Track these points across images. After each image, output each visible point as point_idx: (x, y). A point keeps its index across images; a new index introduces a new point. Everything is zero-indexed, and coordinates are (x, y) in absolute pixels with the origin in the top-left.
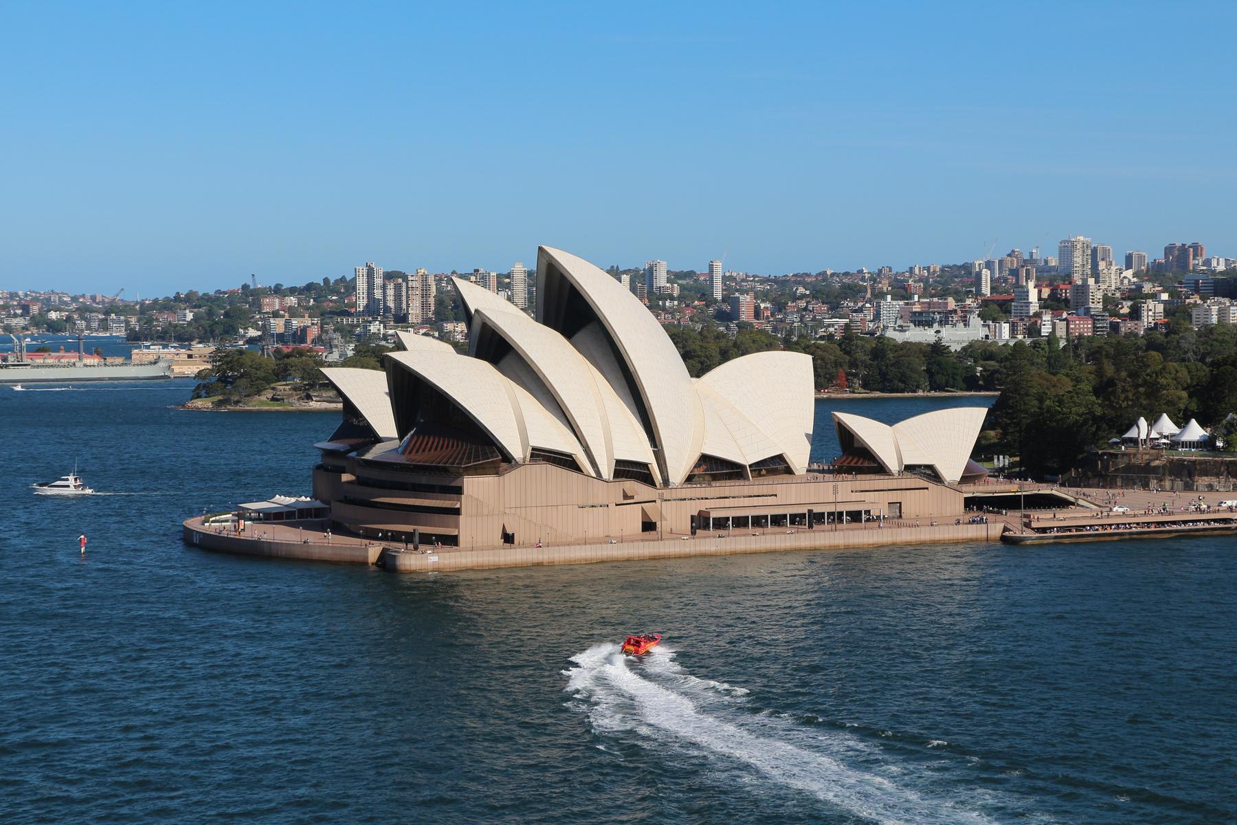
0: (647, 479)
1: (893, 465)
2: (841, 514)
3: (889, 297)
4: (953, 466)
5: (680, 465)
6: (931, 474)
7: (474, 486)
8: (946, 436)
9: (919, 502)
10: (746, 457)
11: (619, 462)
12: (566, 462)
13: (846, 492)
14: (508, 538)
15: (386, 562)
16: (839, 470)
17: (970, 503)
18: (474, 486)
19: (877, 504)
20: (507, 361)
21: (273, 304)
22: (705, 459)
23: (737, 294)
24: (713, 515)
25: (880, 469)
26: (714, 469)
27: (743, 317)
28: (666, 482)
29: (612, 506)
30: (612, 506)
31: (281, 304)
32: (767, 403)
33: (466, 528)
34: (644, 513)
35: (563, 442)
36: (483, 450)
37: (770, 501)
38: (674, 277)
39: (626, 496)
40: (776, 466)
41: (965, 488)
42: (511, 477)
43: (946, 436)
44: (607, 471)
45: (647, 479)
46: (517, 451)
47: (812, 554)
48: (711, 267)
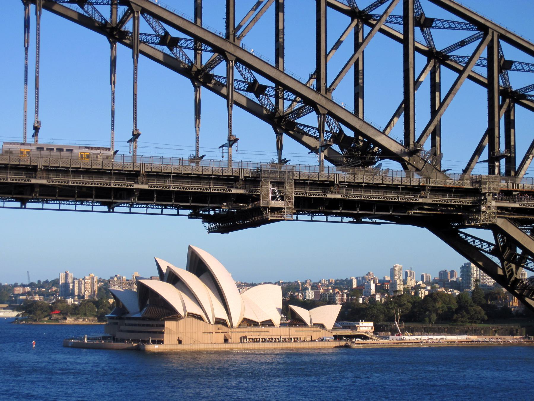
5: (236, 321)
6: (322, 326)
7: (169, 325)
10: (259, 320)
11: (216, 318)
12: (200, 318)
14: (180, 342)
16: (291, 324)
17: (336, 337)
18: (169, 325)
20: (178, 284)
21: (19, 290)
22: (245, 319)
26: (248, 322)
28: (232, 327)
29: (214, 333)
30: (214, 333)
31: (23, 290)
33: (166, 338)
34: (224, 336)
35: (198, 311)
36: (171, 313)
37: (267, 333)
39: (218, 329)
40: (269, 323)
42: (181, 322)
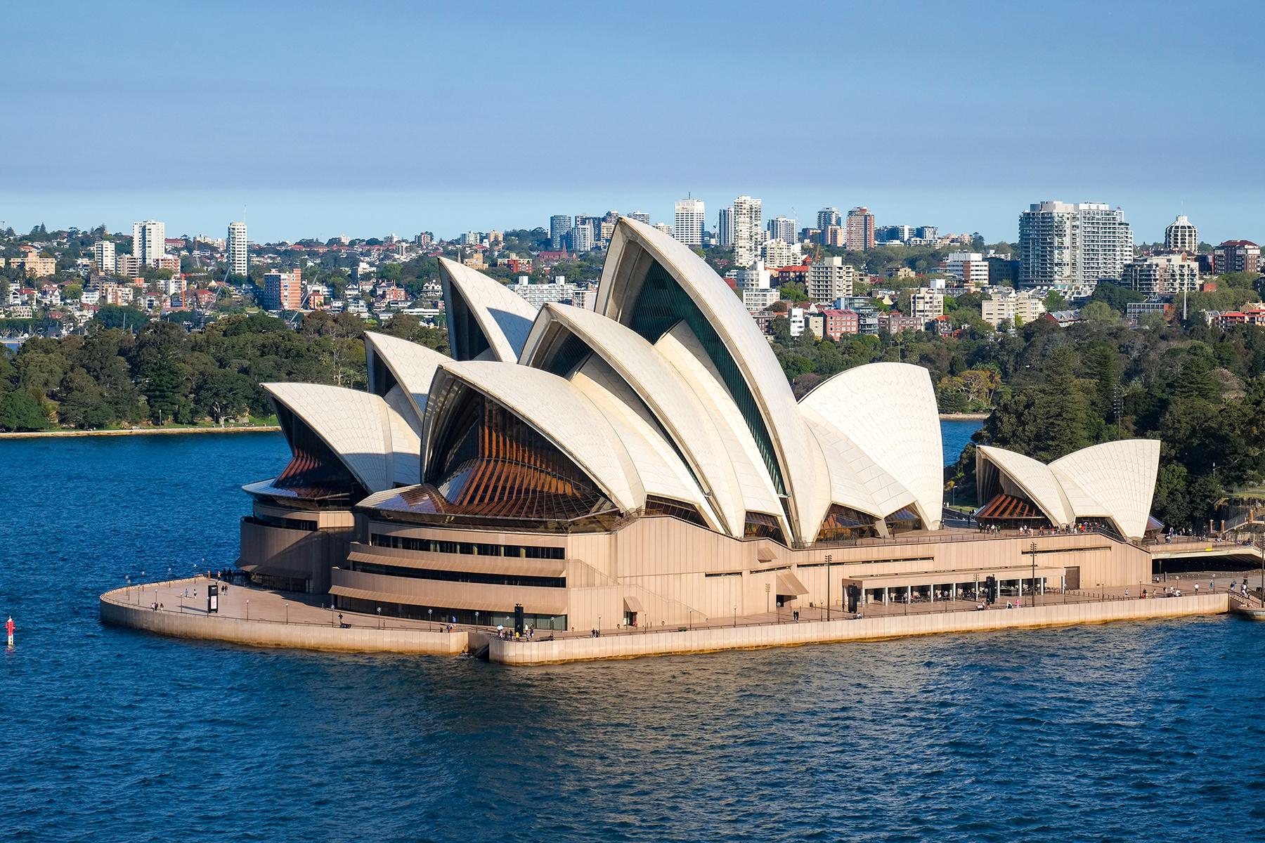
0: (778, 536)
1: (1060, 517)
2: (946, 587)
3: (525, 279)
4: (1134, 517)
8: (1115, 477)
9: (1101, 565)
10: (881, 507)
11: (750, 515)
12: (690, 514)
13: (1000, 554)
15: (480, 655)
19: (1052, 570)
22: (837, 511)
23: (274, 272)
24: (867, 585)
25: (1043, 523)
26: (849, 525)
27: (287, 305)
28: (798, 545)
32: (881, 433)
36: (575, 499)
37: (926, 566)
38: (174, 246)
40: (906, 521)
41: (1151, 548)
43: (1115, 477)
44: (738, 528)
45: (778, 536)
46: (628, 500)
47: (961, 643)
48: (231, 231)
